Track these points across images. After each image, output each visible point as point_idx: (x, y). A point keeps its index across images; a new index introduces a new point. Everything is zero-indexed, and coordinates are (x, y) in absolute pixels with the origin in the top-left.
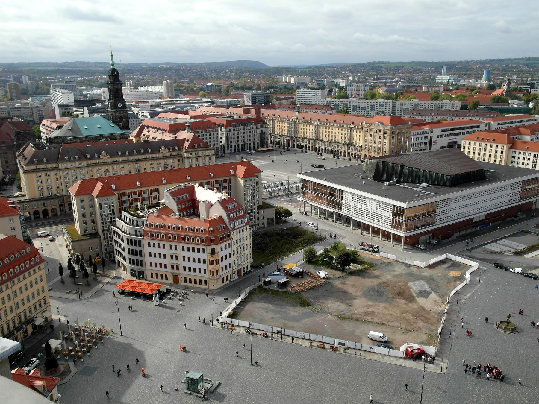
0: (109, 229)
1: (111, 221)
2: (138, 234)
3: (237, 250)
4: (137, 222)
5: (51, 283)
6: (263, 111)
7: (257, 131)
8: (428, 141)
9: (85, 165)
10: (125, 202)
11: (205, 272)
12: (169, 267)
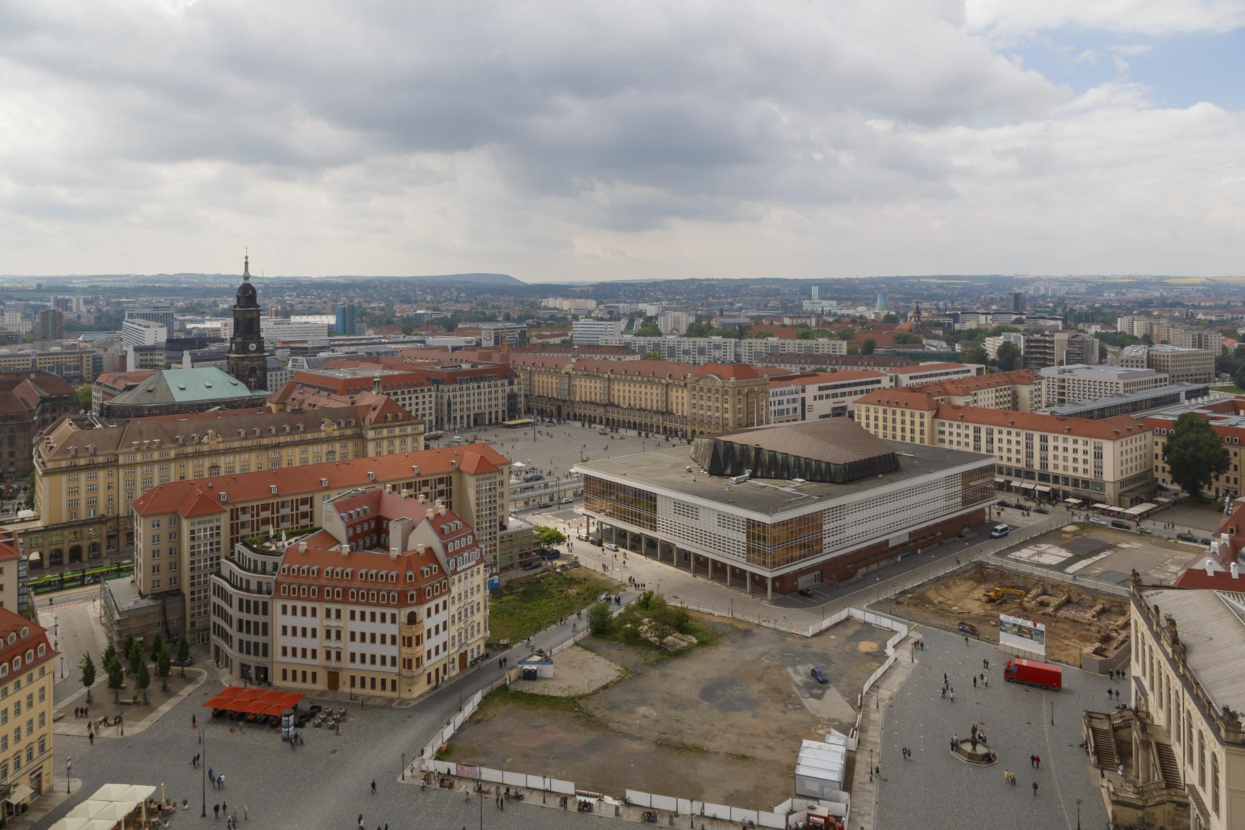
0: (206, 582)
1: (211, 565)
2: (264, 588)
4: (264, 564)
5: (61, 705)
6: (513, 356)
7: (504, 391)
8: (798, 405)
10: (243, 525)
11: (394, 663)
12: (321, 655)
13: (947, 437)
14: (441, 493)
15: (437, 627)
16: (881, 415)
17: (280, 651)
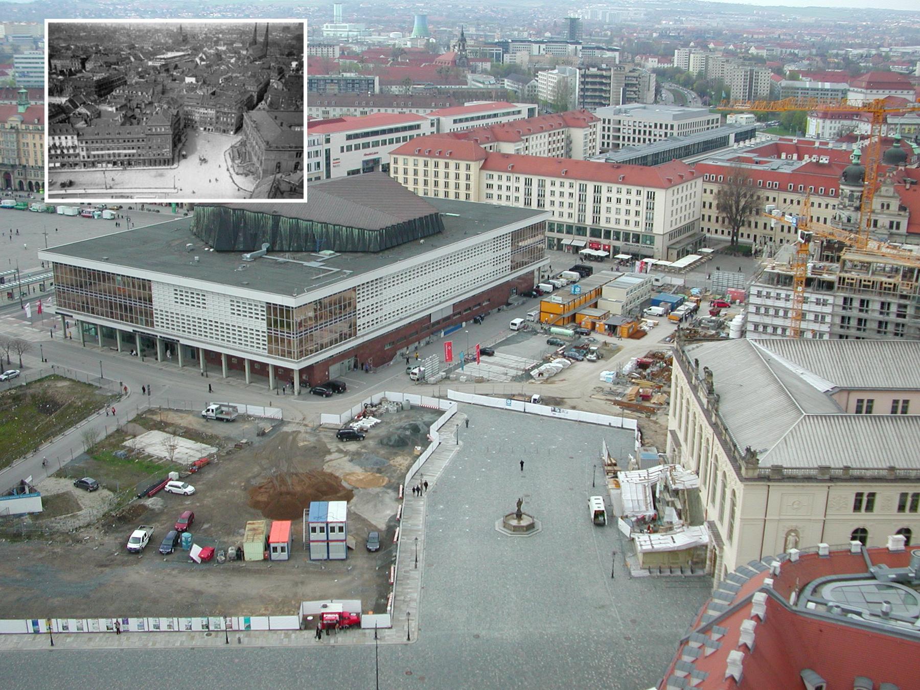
8: (322, 160)
13: (495, 192)
16: (421, 168)
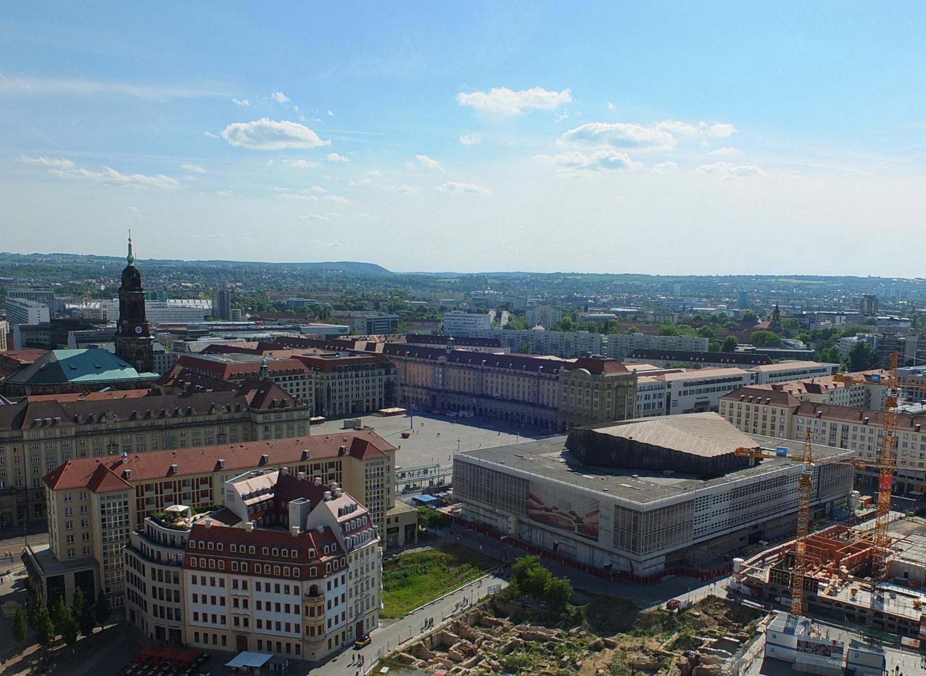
3: (357, 587)
7: (380, 380)
8: (664, 400)
9: (73, 433)
10: (149, 501)
11: (297, 631)
12: (230, 621)
14: (332, 477)
15: (336, 599)
17: (192, 616)
